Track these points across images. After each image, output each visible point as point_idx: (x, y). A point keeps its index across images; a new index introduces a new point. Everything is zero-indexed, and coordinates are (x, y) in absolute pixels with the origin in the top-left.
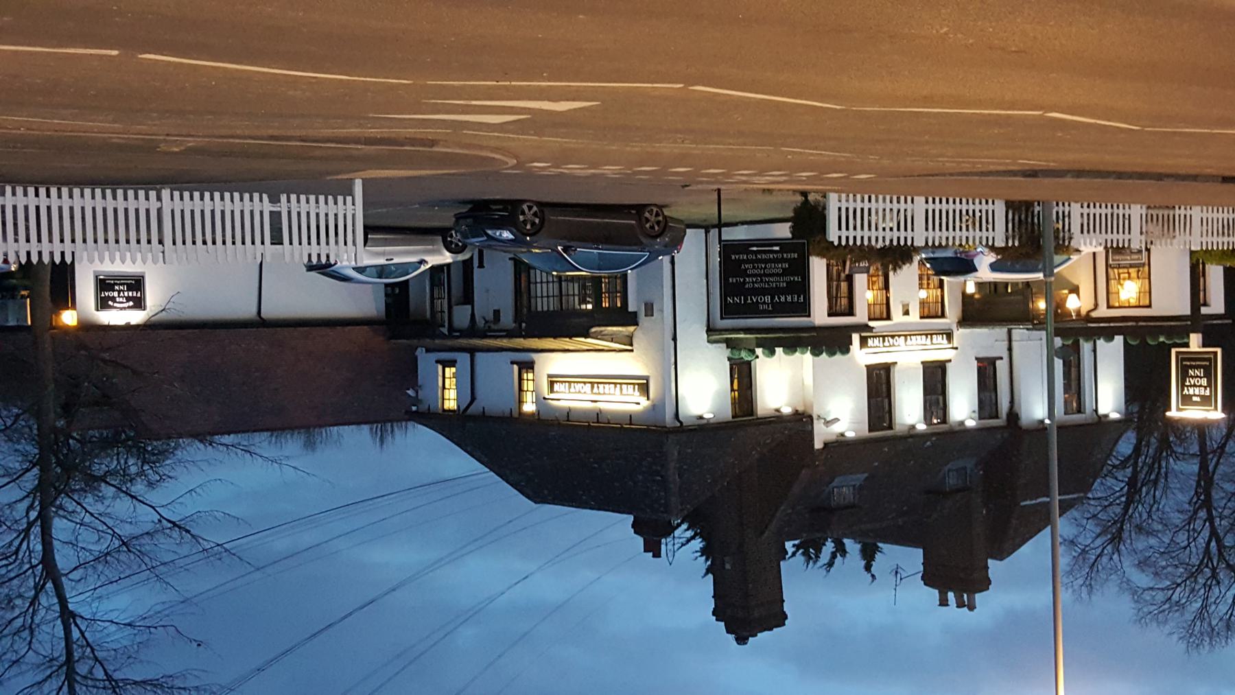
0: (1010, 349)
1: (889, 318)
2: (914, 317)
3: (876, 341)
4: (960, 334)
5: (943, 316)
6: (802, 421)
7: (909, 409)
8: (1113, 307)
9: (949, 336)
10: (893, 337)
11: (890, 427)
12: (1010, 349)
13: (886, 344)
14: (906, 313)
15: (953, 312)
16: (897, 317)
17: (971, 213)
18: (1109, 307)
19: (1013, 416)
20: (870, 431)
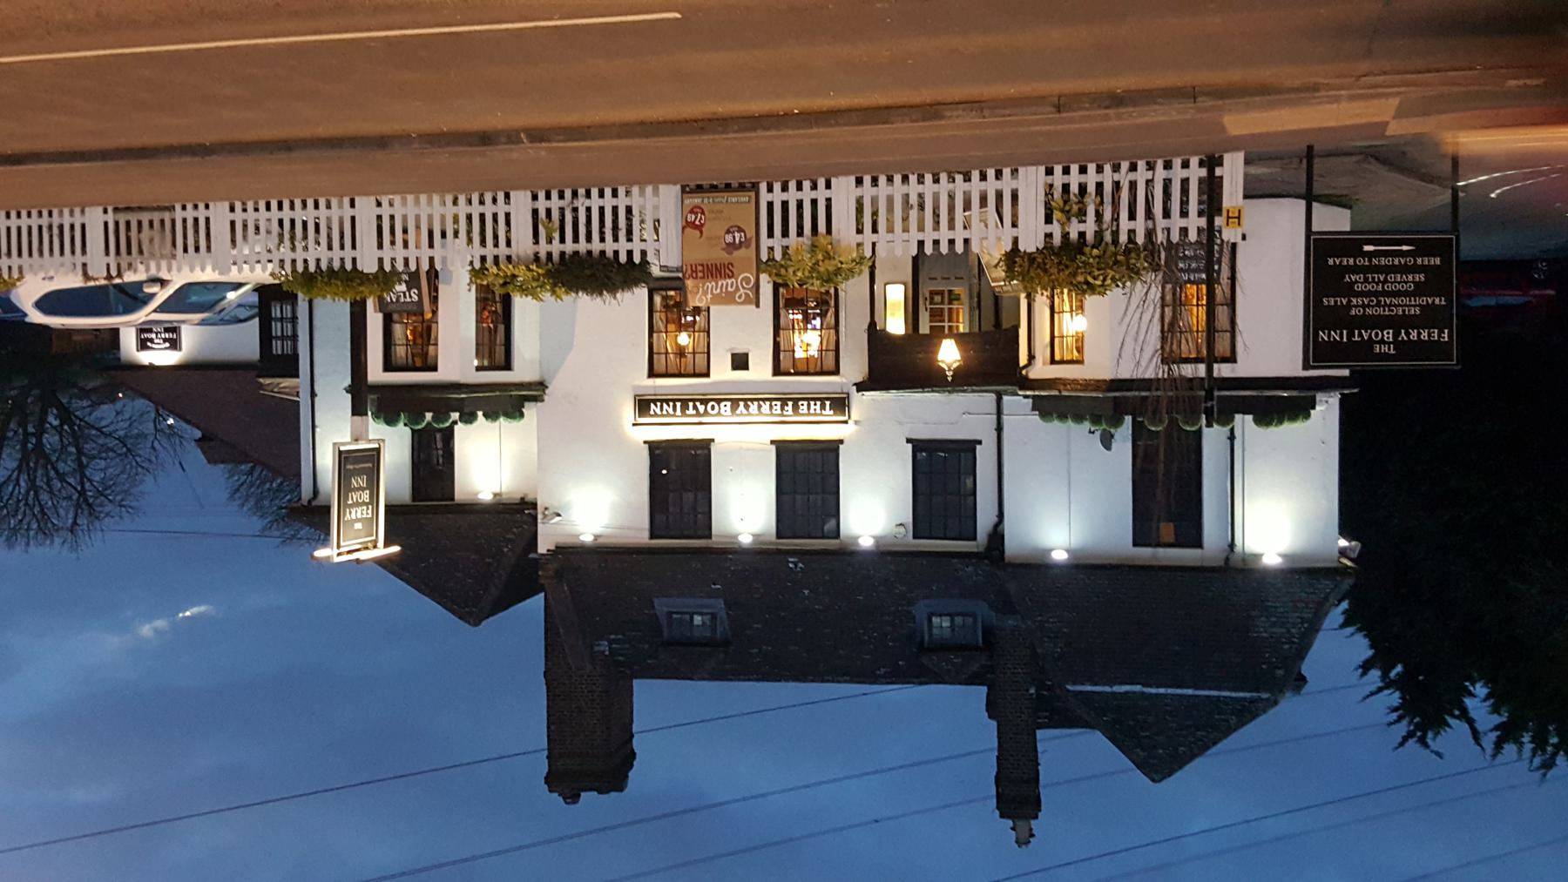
0: (999, 429)
1: (707, 375)
2: (760, 370)
3: (668, 408)
4: (863, 403)
5: (836, 372)
6: (520, 514)
7: (745, 509)
8: (1062, 362)
9: (840, 404)
10: (705, 402)
11: (709, 536)
12: (999, 429)
13: (691, 411)
14: (740, 362)
15: (855, 365)
16: (722, 372)
17: (555, 215)
18: (1053, 361)
19: (997, 535)
20: (652, 536)
